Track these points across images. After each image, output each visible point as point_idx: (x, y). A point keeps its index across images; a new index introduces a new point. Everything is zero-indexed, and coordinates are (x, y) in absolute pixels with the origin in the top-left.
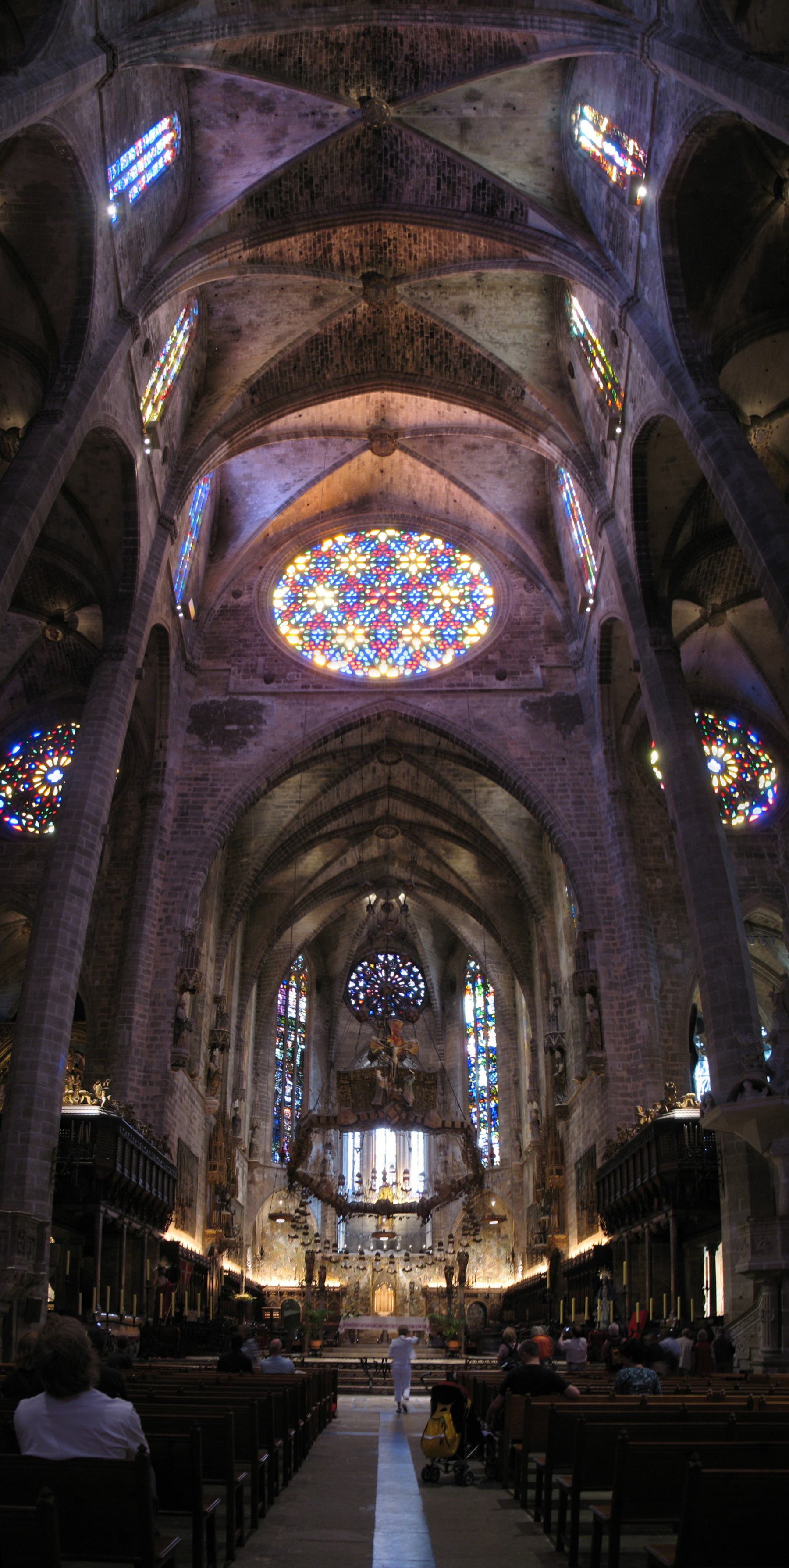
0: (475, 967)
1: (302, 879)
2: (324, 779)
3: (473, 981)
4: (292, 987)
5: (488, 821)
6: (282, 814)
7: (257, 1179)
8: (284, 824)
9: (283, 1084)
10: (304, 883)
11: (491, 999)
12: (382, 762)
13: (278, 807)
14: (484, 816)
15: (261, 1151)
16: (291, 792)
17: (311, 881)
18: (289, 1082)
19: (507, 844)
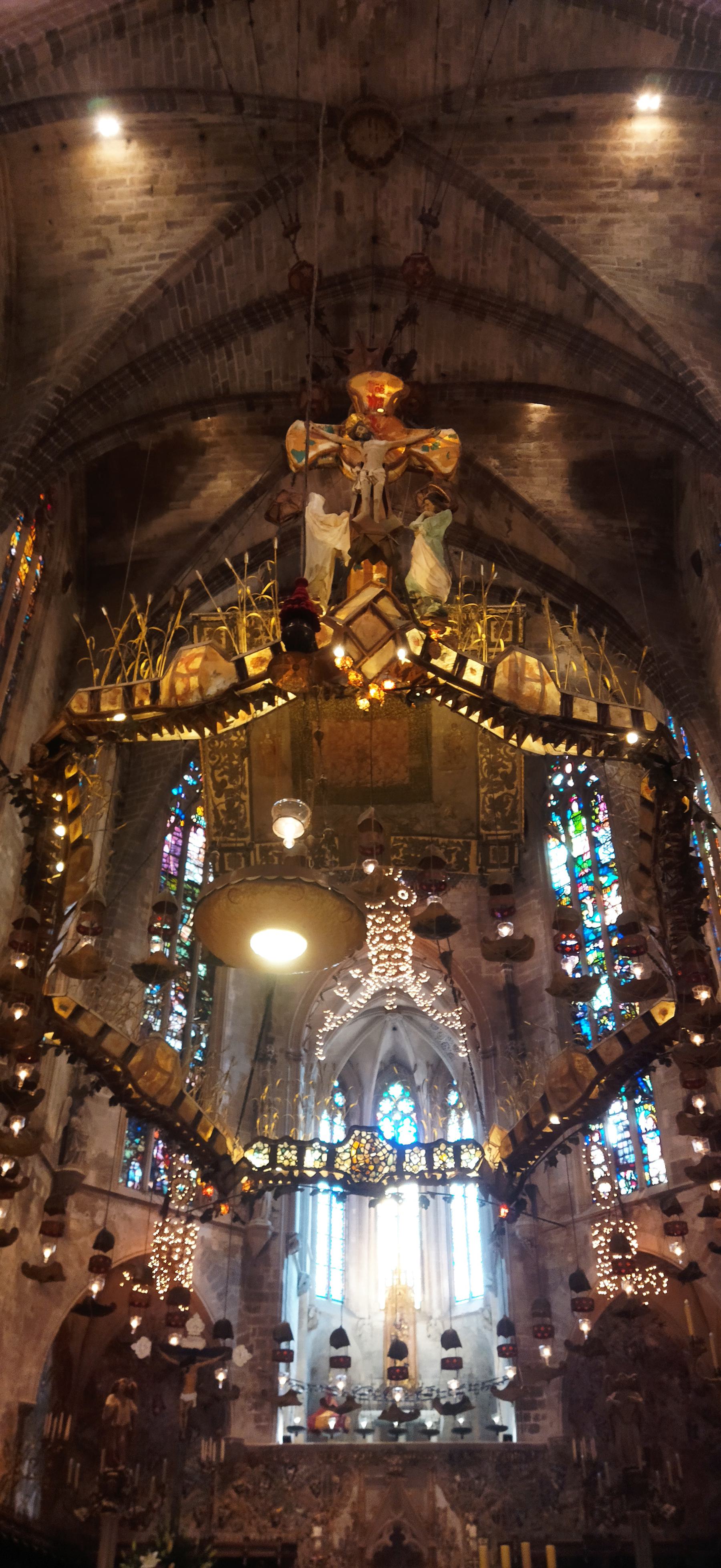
0: (564, 784)
1: (196, 526)
2: (224, 205)
3: (563, 809)
4: (197, 826)
5: (604, 277)
6: (130, 283)
7: (73, 1225)
8: (131, 301)
9: (163, 1012)
10: (200, 534)
11: (603, 834)
12: (354, 157)
13: (119, 272)
14: (593, 268)
15: (92, 1152)
16: (149, 239)
17: (216, 528)
18: (178, 1008)
19: (652, 322)
